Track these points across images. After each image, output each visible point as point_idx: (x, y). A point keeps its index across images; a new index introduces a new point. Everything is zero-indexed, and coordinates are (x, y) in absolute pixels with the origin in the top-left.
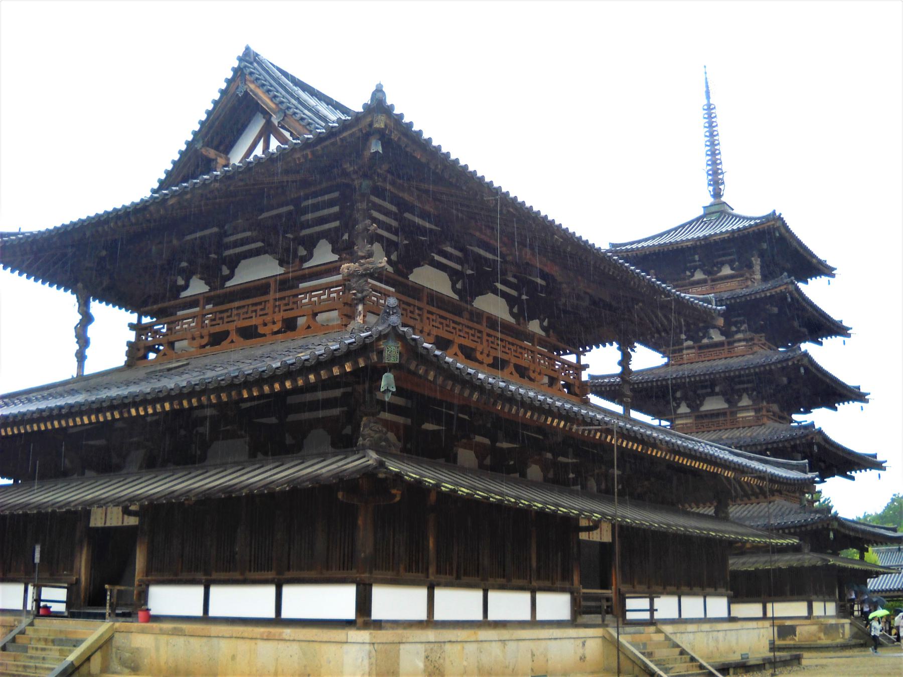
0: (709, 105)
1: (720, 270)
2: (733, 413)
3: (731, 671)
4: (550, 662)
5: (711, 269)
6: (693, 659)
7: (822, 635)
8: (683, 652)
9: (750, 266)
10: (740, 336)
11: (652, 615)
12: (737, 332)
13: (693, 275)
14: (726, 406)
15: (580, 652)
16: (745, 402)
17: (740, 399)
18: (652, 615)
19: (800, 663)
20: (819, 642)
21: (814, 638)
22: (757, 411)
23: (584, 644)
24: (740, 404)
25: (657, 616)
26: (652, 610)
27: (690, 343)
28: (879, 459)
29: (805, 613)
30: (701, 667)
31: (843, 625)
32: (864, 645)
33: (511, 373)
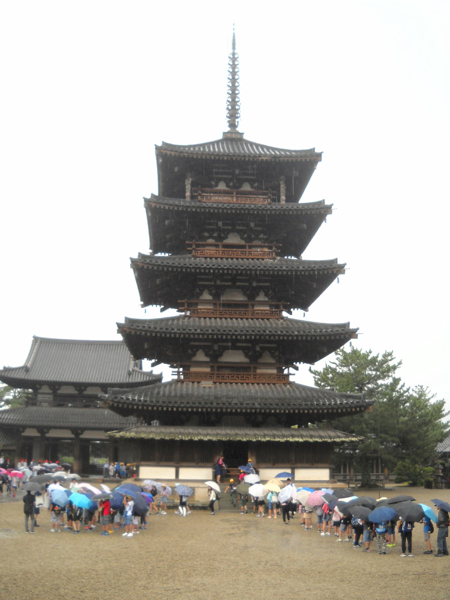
29: (173, 477)
32: (234, 507)
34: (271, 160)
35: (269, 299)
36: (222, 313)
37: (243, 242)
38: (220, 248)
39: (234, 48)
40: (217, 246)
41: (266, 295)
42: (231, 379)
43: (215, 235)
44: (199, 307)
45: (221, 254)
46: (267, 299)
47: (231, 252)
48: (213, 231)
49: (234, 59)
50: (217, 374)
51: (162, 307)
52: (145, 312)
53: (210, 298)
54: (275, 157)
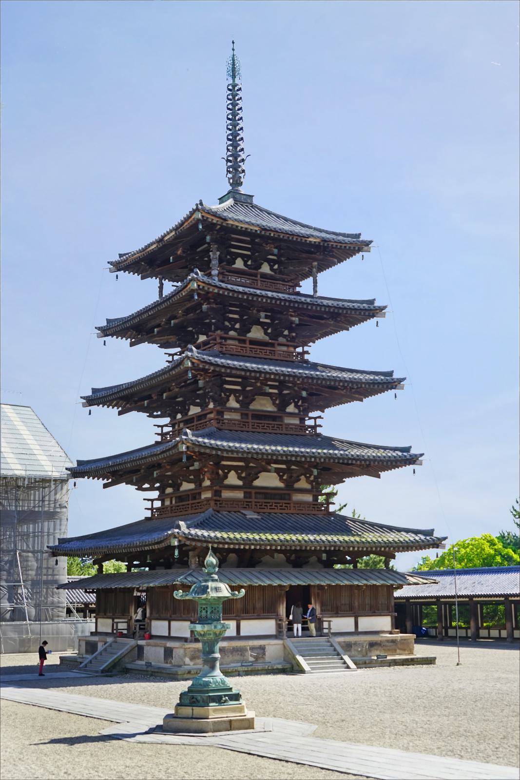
34: (319, 243)
35: (300, 411)
36: (264, 426)
37: (267, 338)
38: (248, 345)
39: (234, 77)
40: (240, 341)
41: (296, 406)
42: (270, 509)
43: (237, 326)
44: (225, 417)
45: (248, 352)
46: (297, 411)
47: (258, 350)
48: (236, 321)
49: (234, 92)
50: (256, 502)
51: (120, 409)
52: (90, 414)
53: (237, 405)
54: (324, 240)
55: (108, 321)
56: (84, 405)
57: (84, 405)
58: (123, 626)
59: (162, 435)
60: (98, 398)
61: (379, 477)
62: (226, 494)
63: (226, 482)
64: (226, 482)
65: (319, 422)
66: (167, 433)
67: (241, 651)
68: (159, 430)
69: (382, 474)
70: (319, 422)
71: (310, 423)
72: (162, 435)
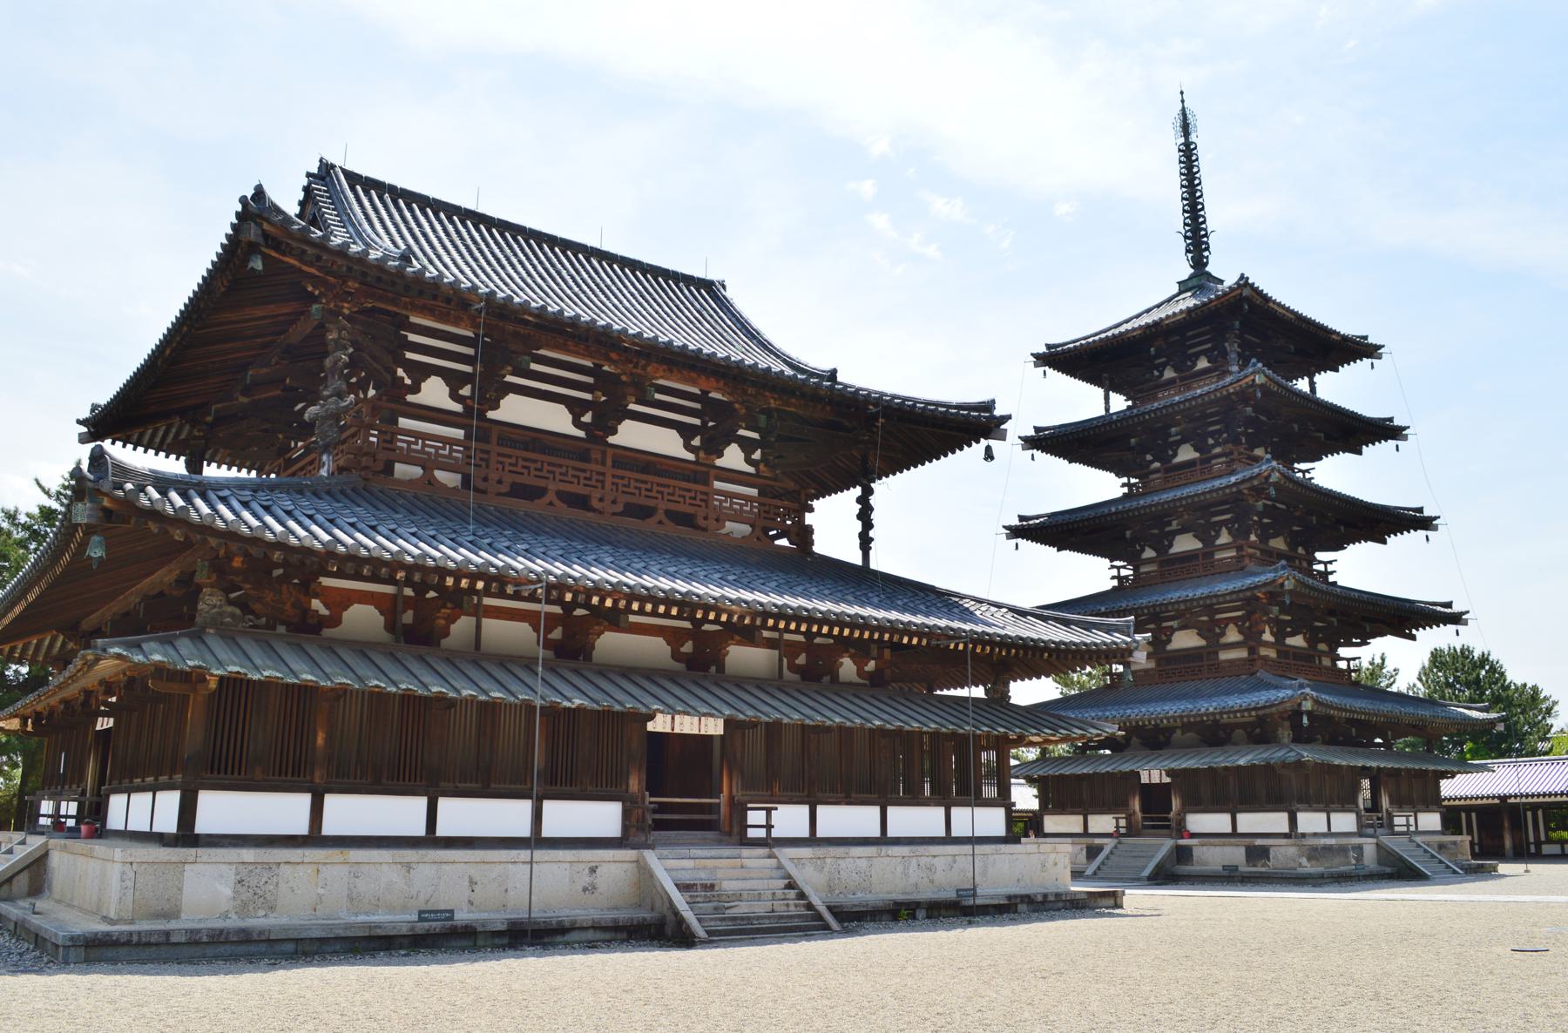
0: (1187, 144)
1: (1195, 365)
2: (1212, 554)
3: (921, 914)
4: (511, 893)
5: (1184, 365)
6: (802, 895)
7: (1304, 861)
8: (791, 886)
9: (1224, 354)
10: (1218, 450)
11: (769, 832)
12: (1214, 446)
13: (1162, 375)
14: (1199, 545)
15: (586, 880)
16: (1225, 538)
17: (1218, 536)
18: (769, 832)
19: (1119, 906)
20: (1300, 870)
21: (1293, 865)
22: (1239, 549)
23: (593, 870)
24: (1219, 542)
25: (775, 833)
26: (769, 827)
27: (1157, 465)
28: (1456, 608)
30: (810, 906)
31: (1359, 848)
33: (660, 522)
55: (1037, 429)
56: (1009, 537)
57: (1009, 537)
58: (1123, 823)
59: (1118, 577)
60: (1029, 530)
61: (1413, 638)
62: (1263, 652)
63: (1223, 640)
64: (1223, 640)
65: (1330, 567)
66: (1126, 577)
67: (1342, 850)
68: (1114, 572)
69: (1420, 633)
70: (1330, 567)
71: (1321, 567)
72: (1118, 577)
